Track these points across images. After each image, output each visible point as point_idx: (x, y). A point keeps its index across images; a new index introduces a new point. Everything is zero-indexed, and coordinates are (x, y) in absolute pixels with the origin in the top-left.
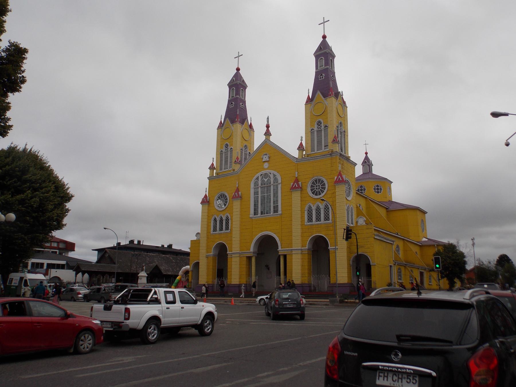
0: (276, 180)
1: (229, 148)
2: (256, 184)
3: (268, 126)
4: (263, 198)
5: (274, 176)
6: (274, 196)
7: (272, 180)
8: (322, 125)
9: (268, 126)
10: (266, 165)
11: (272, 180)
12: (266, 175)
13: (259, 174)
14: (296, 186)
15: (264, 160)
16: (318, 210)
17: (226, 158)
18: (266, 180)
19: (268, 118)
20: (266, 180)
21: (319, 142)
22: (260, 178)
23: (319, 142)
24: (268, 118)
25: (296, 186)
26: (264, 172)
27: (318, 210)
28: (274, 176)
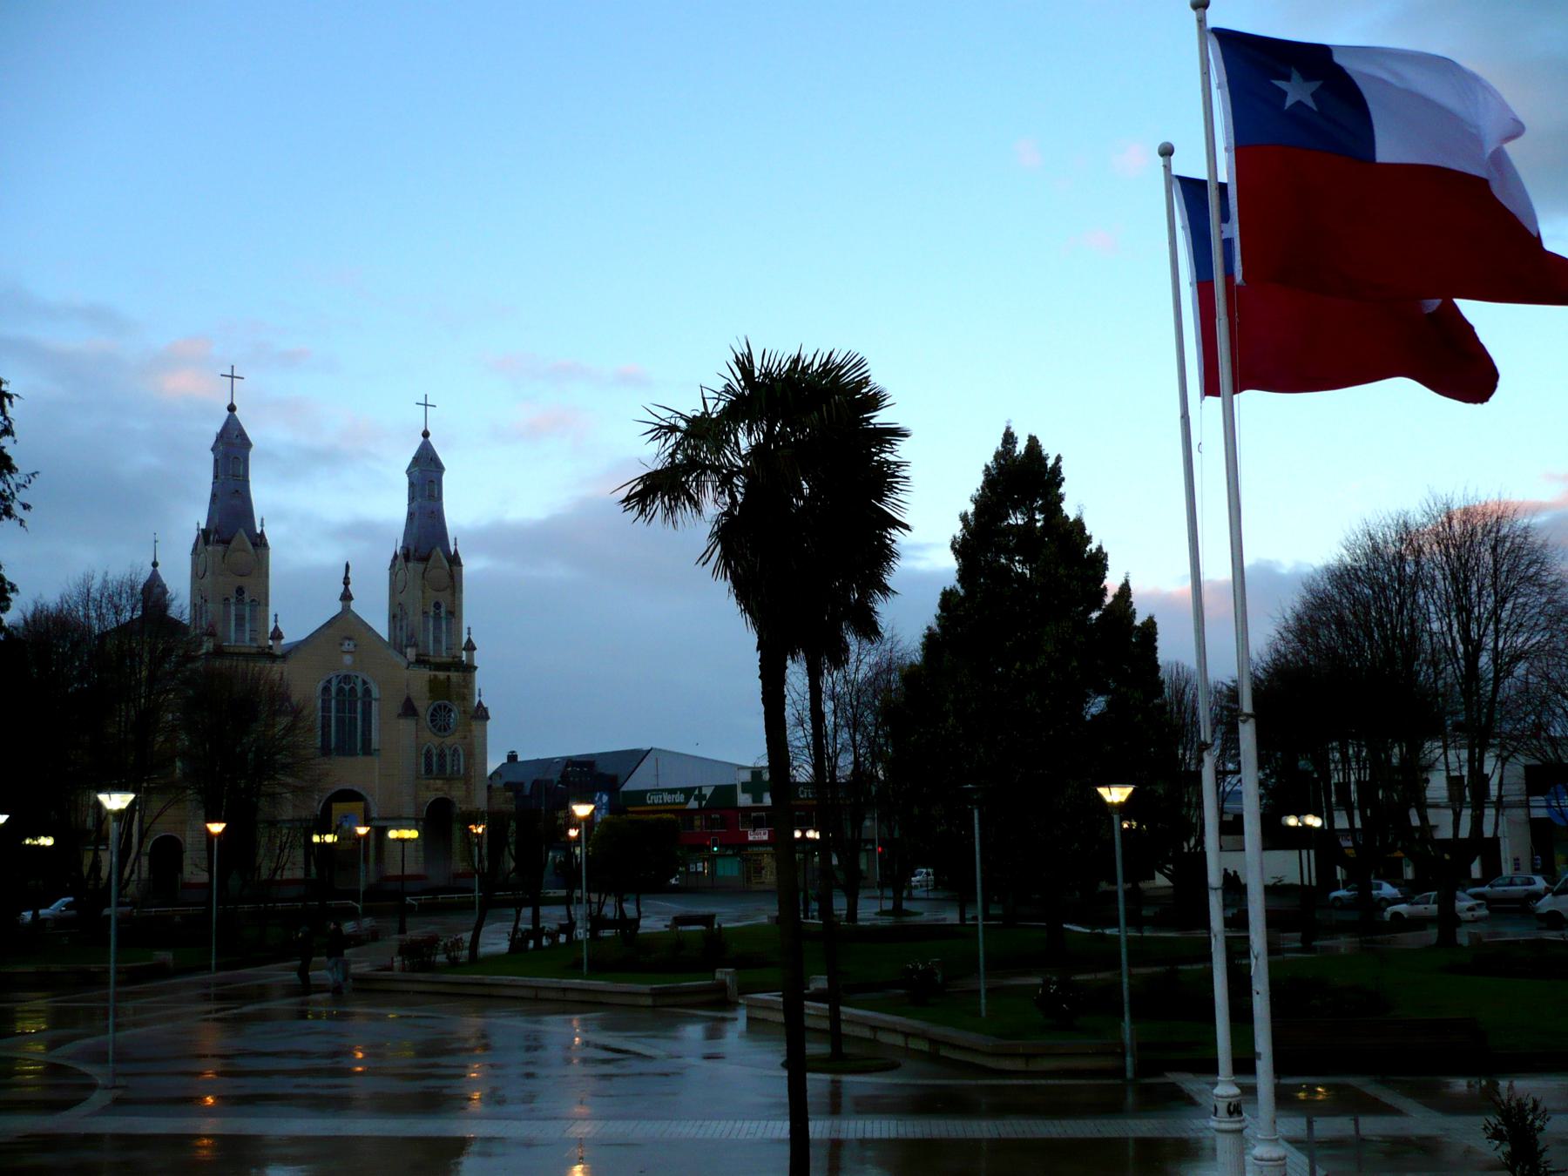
0: (367, 692)
1: (247, 599)
2: (326, 689)
3: (346, 582)
4: (340, 721)
5: (364, 682)
6: (364, 720)
7: (359, 689)
8: (443, 610)
9: (346, 582)
10: (348, 659)
11: (359, 689)
12: (347, 679)
13: (332, 674)
14: (409, 709)
15: (345, 648)
16: (442, 756)
17: (240, 619)
18: (347, 688)
19: (347, 566)
20: (347, 688)
21: (437, 640)
22: (334, 682)
23: (437, 640)
24: (347, 566)
25: (409, 709)
26: (344, 672)
27: (442, 756)
28: (364, 682)
